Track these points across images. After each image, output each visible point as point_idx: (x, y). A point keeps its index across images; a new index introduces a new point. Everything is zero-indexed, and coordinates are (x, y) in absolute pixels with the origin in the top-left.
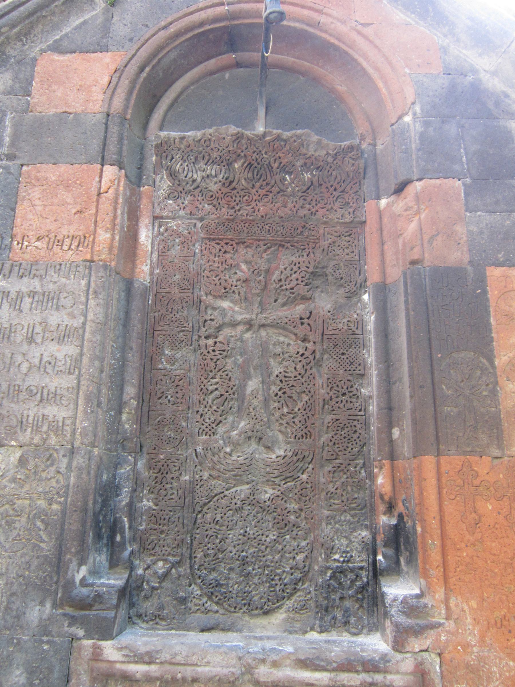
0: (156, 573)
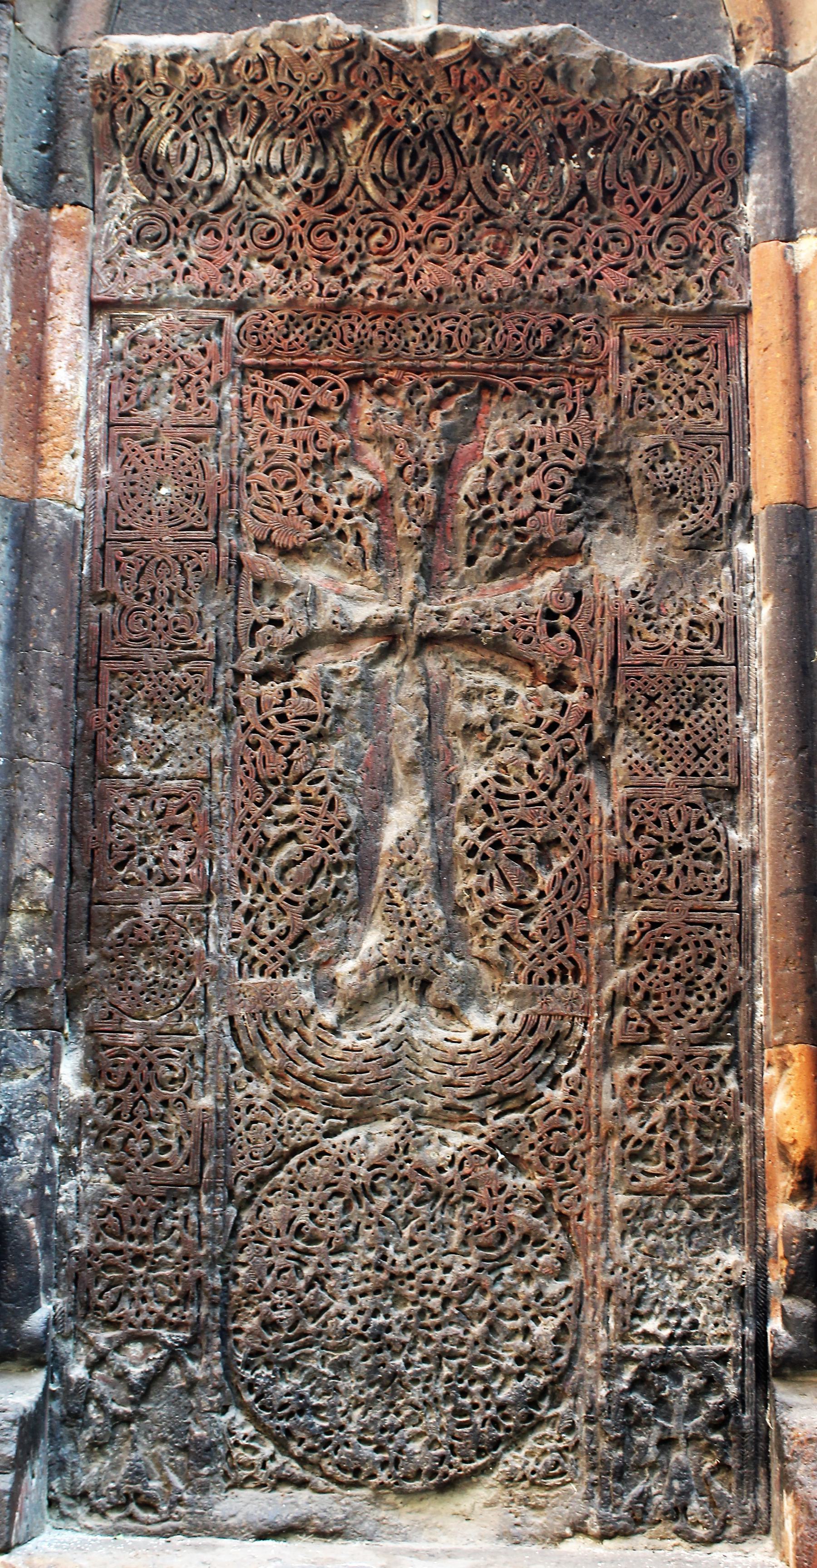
0: (122, 1376)
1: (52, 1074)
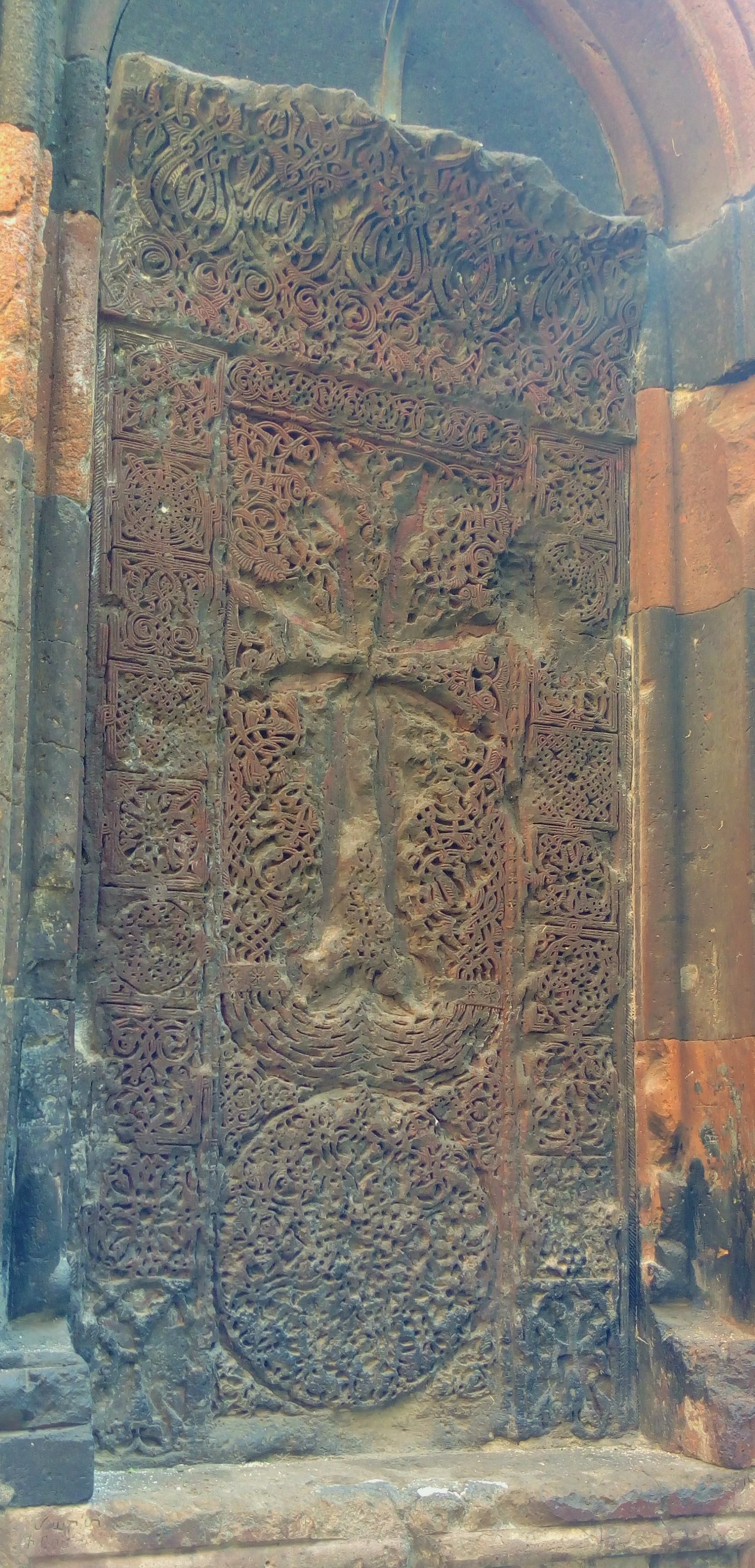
0: (128, 1321)
1: (68, 1043)
